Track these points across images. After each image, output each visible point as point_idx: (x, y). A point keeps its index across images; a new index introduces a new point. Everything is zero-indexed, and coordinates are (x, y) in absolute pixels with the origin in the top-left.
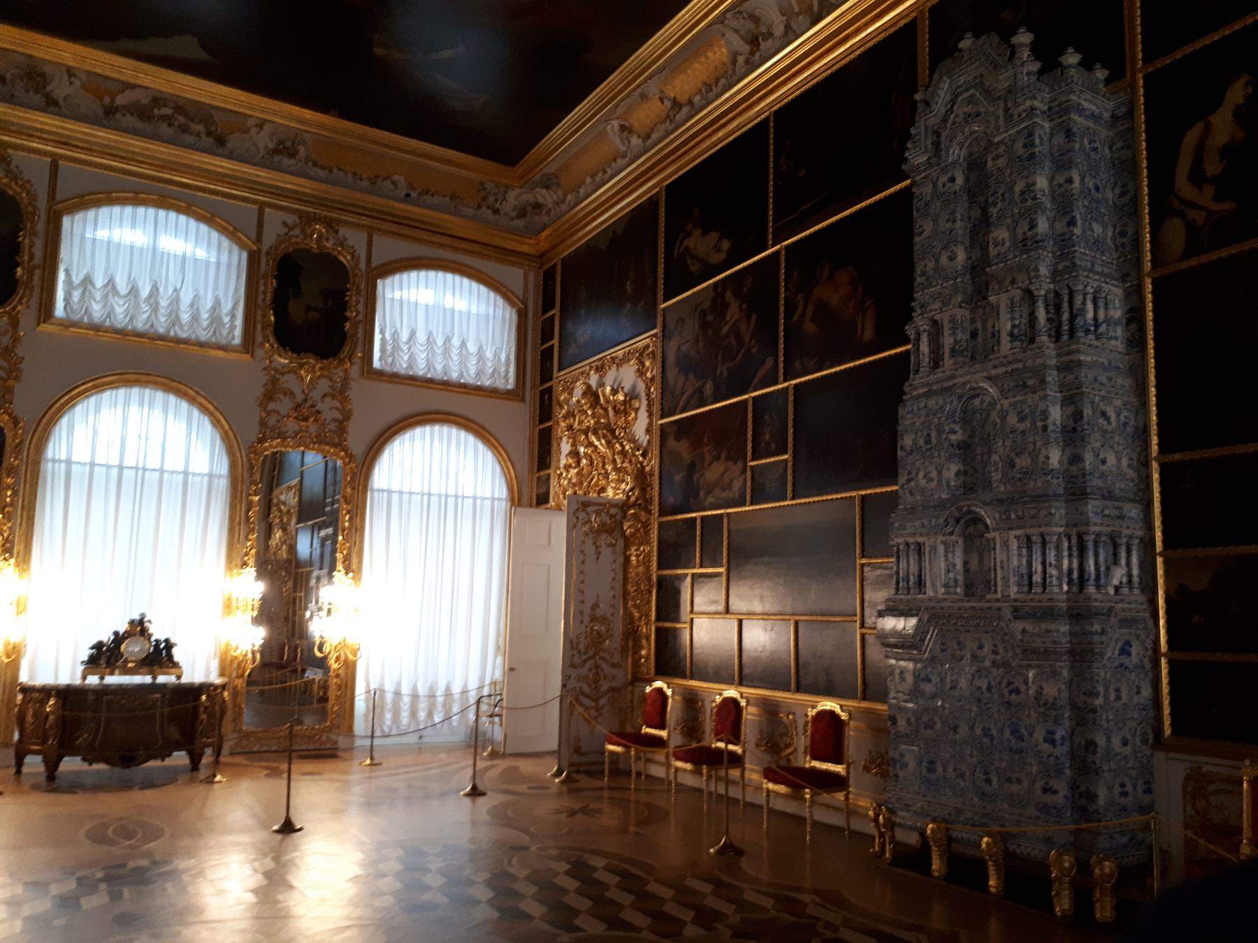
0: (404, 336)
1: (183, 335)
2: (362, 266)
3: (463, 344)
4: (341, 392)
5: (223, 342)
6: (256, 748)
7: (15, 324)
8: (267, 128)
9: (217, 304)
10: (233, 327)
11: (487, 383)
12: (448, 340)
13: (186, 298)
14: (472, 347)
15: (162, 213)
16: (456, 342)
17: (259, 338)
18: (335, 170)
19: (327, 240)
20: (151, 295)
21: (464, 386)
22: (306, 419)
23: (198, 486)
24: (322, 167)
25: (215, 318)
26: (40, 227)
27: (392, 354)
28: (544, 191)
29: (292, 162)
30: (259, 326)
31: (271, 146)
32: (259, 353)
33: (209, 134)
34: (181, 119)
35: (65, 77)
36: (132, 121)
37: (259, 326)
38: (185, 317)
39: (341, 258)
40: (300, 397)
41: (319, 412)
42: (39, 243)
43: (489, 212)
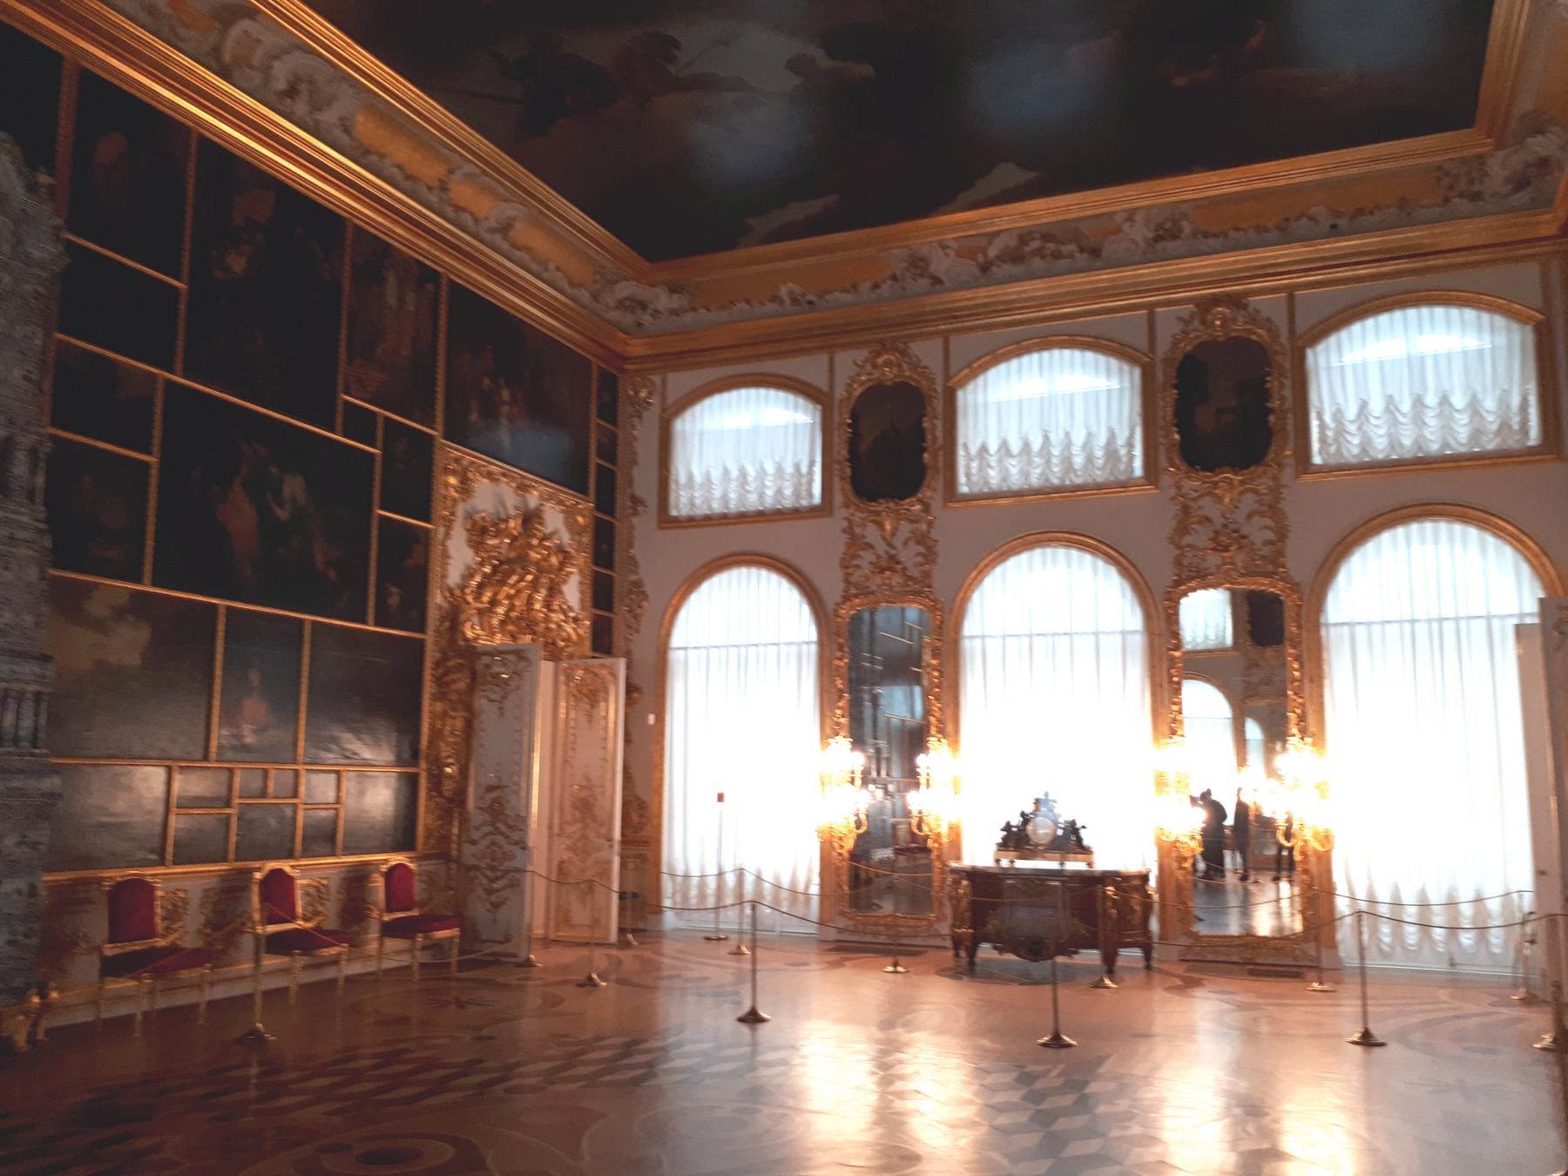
0: (1351, 412)
1: (1079, 481)
2: (1284, 339)
3: (1445, 400)
4: (1273, 509)
5: (1122, 478)
6: (1210, 957)
7: (927, 508)
8: (1139, 218)
9: (1112, 437)
10: (1131, 458)
11: (1491, 446)
12: (1418, 402)
13: (1078, 438)
14: (1459, 401)
15: (1046, 354)
16: (1431, 400)
17: (1163, 459)
18: (1231, 233)
19: (1234, 321)
20: (1042, 448)
21: (1456, 459)
22: (1226, 549)
23: (1111, 645)
24: (1215, 235)
25: (1111, 453)
26: (940, 409)
27: (1336, 440)
28: (1540, 138)
29: (1178, 243)
30: (1162, 449)
31: (1151, 235)
32: (1166, 480)
33: (1082, 250)
34: (1052, 246)
35: (940, 251)
36: (1008, 268)
37: (1162, 449)
38: (1078, 461)
39: (1254, 337)
40: (1219, 521)
41: (1244, 537)
42: (939, 423)
43: (1465, 201)
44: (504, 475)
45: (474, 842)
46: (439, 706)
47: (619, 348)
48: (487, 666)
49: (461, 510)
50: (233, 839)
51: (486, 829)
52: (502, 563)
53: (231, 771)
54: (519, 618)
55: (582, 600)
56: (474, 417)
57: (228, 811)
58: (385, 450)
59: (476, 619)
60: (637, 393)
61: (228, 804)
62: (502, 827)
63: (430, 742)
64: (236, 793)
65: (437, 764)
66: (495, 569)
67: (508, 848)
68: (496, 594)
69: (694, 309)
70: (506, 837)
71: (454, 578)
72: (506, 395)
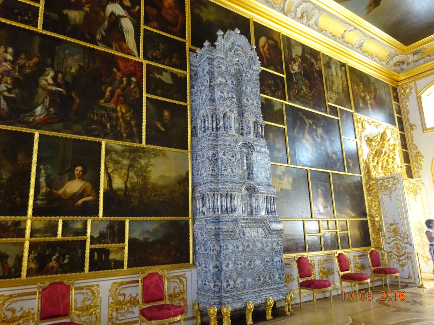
44: (373, 122)
45: (389, 243)
46: (369, 198)
47: (396, 78)
48: (382, 183)
49: (363, 134)
50: (323, 244)
51: (392, 239)
52: (377, 150)
53: (319, 221)
54: (386, 168)
55: (401, 160)
56: (361, 105)
57: (320, 234)
58: (341, 117)
59: (373, 170)
60: (405, 91)
61: (320, 232)
62: (399, 238)
63: (369, 210)
64: (321, 229)
66: (376, 153)
67: (403, 245)
68: (378, 160)
69: (423, 58)
70: (402, 241)
71: (365, 157)
72: (368, 97)
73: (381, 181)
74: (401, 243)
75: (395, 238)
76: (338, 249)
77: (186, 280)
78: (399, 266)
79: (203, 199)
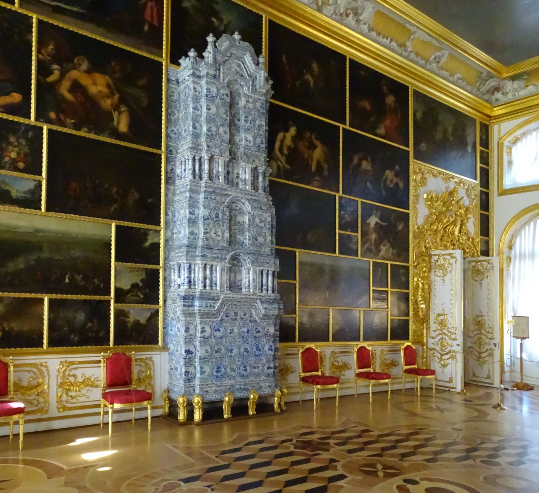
45: (433, 338)
48: (437, 261)
51: (438, 332)
65: (416, 302)
73: (436, 258)
74: (447, 338)
75: (440, 332)
76: (359, 340)
77: (153, 364)
78: (440, 366)
79: (179, 268)
